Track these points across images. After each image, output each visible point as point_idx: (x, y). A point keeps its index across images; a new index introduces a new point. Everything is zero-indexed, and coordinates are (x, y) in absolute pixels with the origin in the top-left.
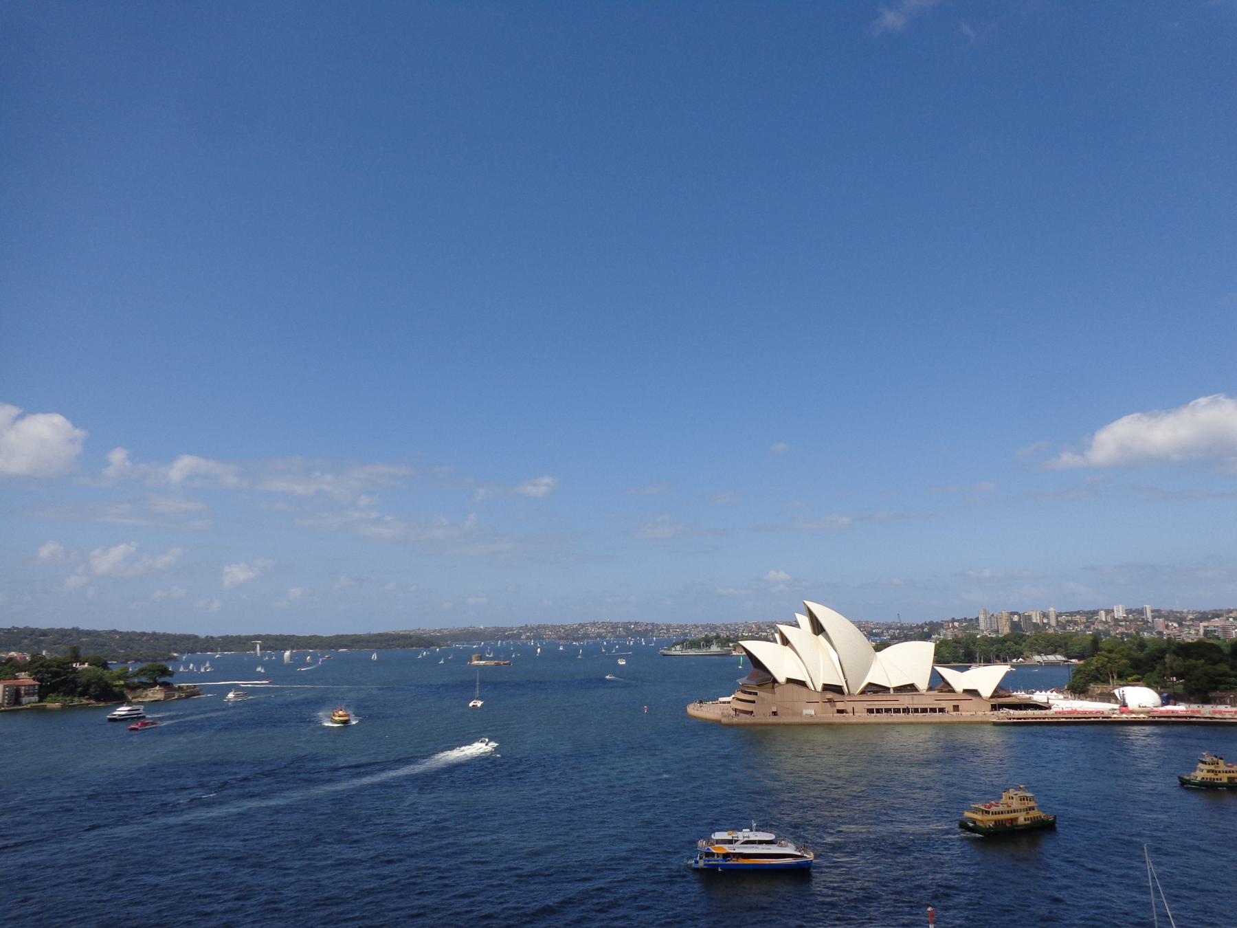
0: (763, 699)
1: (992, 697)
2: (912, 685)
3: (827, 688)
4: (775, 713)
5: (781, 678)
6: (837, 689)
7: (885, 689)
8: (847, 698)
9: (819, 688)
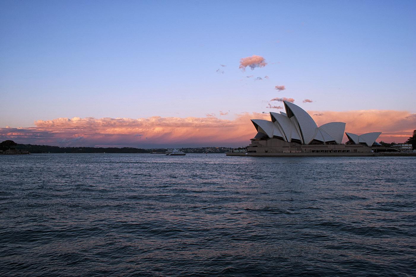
0: (261, 145)
1: (373, 146)
3: (293, 141)
4: (266, 152)
5: (270, 136)
6: (298, 142)
7: (321, 143)
8: (302, 146)
9: (289, 140)
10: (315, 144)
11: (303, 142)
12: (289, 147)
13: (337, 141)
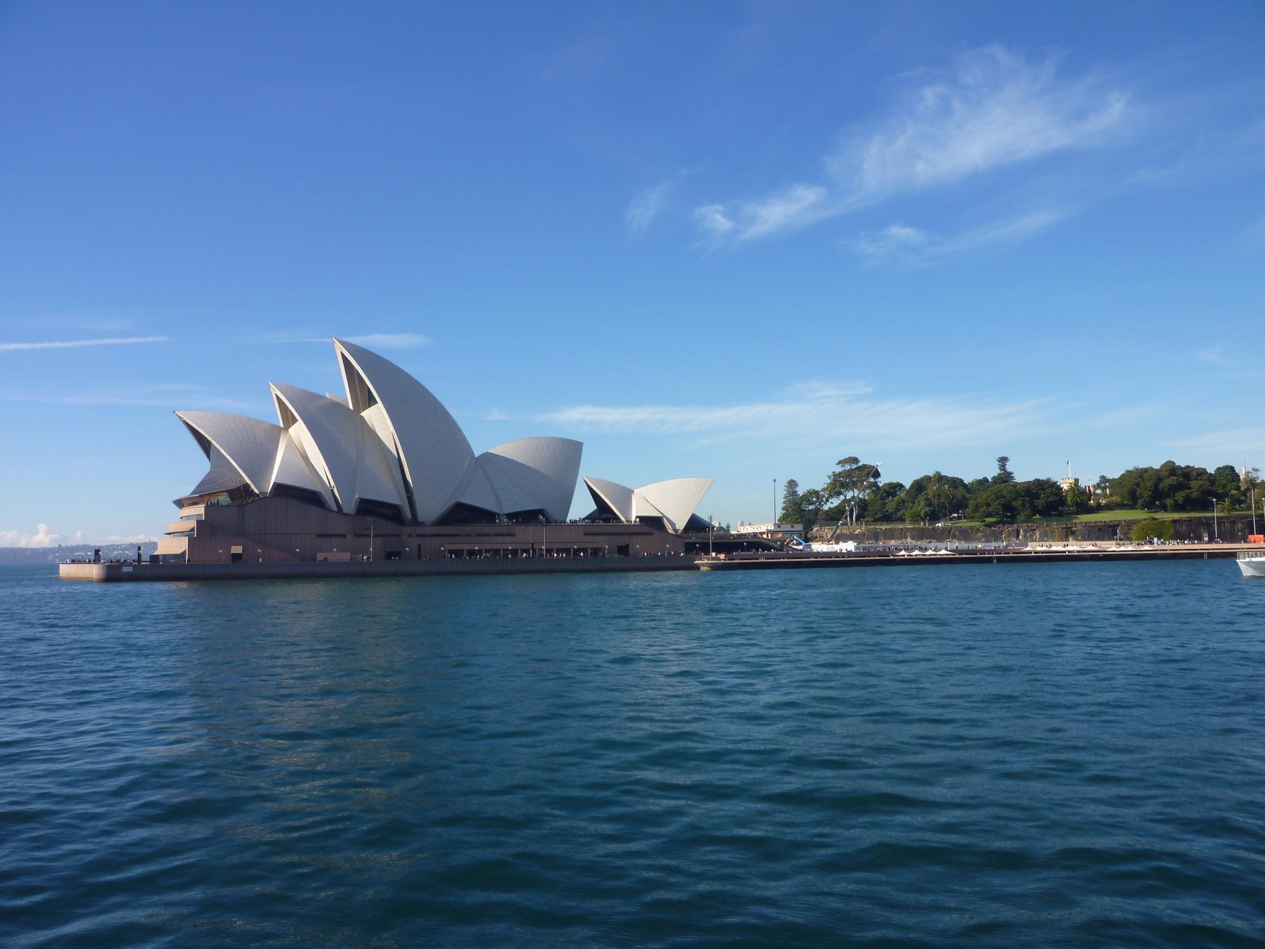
2: (541, 512)
3: (368, 507)
6: (389, 513)
8: (408, 530)
9: (350, 508)
10: (464, 521)
11: (408, 514)
12: (343, 536)
13: (553, 512)
